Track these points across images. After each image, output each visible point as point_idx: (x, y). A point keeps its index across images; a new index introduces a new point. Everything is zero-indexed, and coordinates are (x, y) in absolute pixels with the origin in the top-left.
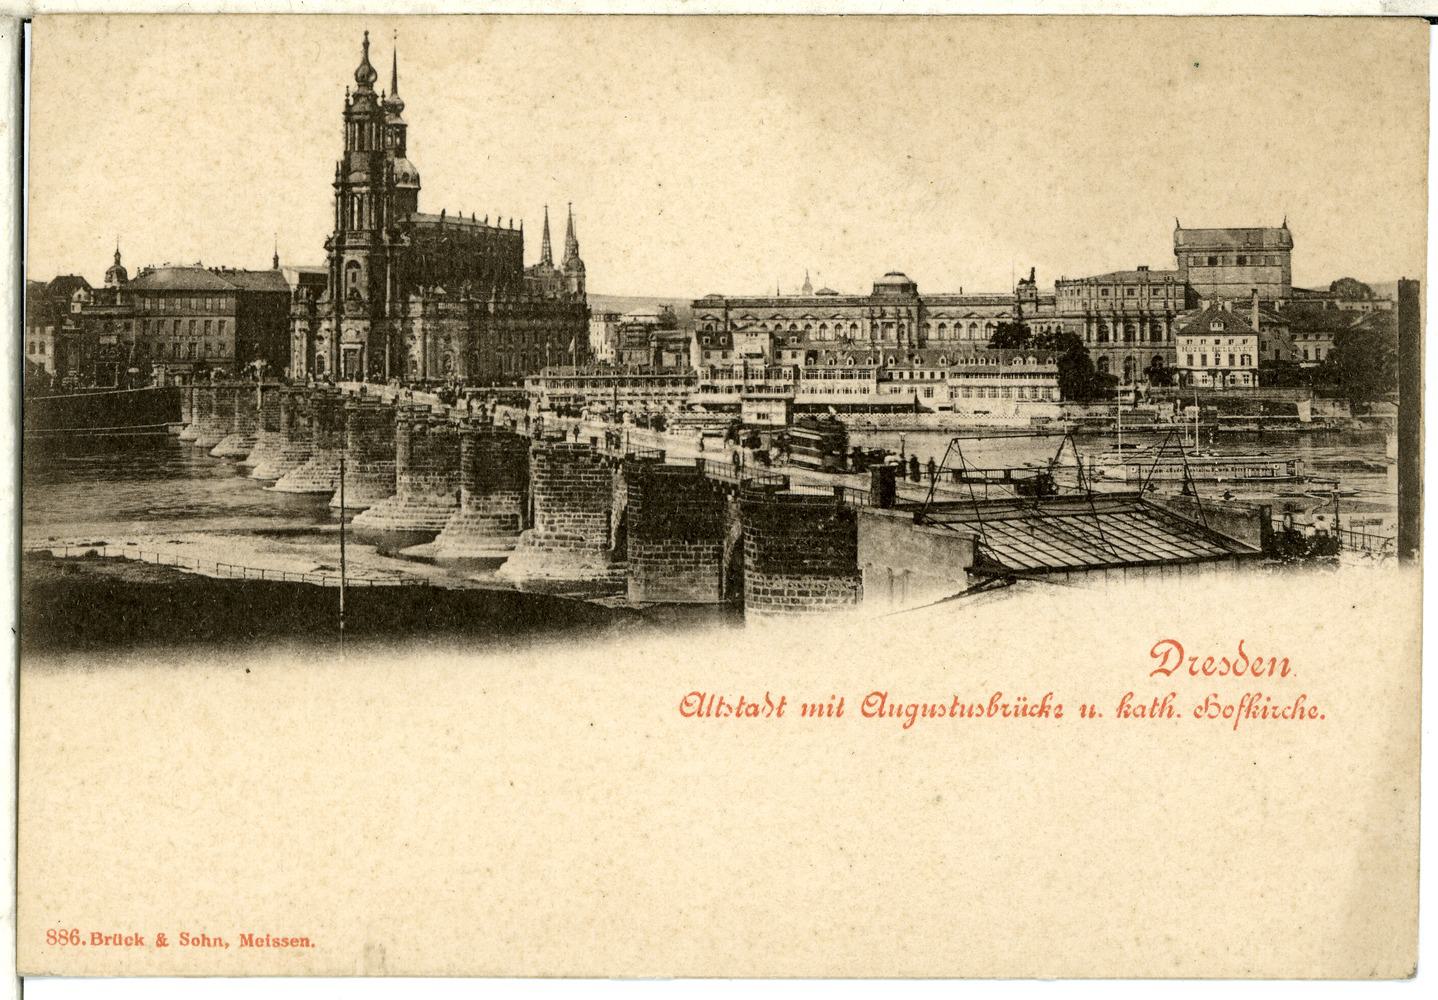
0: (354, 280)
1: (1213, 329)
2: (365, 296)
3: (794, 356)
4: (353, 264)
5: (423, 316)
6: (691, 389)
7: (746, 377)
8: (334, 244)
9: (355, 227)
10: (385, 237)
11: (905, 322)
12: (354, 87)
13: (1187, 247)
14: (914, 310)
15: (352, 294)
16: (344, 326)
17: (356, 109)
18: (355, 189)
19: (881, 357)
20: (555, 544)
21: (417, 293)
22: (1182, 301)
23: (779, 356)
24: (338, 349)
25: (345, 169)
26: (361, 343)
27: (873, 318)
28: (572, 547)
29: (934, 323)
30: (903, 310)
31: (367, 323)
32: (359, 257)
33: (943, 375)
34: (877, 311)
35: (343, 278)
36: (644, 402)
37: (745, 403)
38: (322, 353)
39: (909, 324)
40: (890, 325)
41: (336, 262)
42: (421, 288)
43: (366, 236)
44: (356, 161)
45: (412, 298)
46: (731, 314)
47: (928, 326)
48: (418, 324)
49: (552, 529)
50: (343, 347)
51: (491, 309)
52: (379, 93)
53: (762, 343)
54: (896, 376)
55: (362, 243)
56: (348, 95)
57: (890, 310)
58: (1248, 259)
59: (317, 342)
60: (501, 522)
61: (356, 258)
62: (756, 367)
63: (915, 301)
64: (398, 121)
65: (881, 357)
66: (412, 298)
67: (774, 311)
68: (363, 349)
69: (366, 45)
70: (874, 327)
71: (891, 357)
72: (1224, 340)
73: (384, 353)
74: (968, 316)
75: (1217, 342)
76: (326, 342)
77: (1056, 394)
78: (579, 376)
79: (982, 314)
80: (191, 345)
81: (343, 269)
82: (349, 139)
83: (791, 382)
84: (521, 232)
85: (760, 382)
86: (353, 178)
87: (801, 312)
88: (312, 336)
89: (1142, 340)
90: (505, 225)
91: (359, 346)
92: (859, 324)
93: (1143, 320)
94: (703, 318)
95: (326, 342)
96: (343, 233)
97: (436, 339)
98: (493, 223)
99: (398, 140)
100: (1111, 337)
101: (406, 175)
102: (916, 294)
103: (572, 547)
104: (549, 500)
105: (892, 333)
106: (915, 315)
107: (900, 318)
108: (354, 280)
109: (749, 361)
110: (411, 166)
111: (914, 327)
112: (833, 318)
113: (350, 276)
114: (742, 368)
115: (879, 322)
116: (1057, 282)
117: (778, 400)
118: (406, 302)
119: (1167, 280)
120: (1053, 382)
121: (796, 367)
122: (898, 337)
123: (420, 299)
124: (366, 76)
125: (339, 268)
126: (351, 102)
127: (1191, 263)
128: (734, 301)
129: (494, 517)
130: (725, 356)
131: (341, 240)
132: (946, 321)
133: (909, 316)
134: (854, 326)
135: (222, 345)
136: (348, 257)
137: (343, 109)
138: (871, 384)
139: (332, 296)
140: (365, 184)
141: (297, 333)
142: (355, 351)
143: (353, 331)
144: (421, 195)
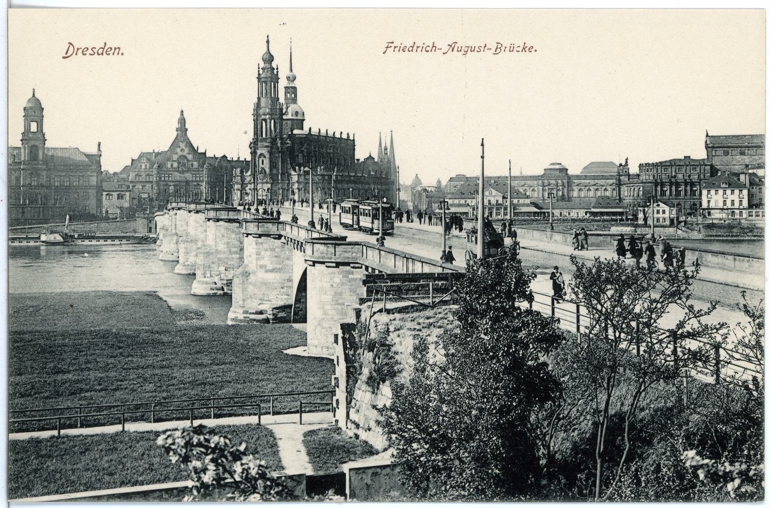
2: (268, 171)
8: (252, 145)
12: (262, 65)
17: (263, 76)
21: (295, 170)
25: (258, 106)
31: (269, 186)
32: (265, 151)
39: (563, 189)
41: (254, 153)
42: (297, 168)
45: (293, 173)
52: (275, 67)
61: (263, 152)
69: (268, 42)
76: (250, 196)
81: (257, 159)
82: (260, 93)
84: (354, 140)
86: (261, 111)
90: (344, 136)
96: (257, 139)
99: (293, 95)
102: (567, 174)
106: (566, 185)
113: (261, 161)
119: (700, 163)
125: (255, 157)
133: (563, 185)
136: (259, 152)
137: (257, 76)
144: (304, 122)
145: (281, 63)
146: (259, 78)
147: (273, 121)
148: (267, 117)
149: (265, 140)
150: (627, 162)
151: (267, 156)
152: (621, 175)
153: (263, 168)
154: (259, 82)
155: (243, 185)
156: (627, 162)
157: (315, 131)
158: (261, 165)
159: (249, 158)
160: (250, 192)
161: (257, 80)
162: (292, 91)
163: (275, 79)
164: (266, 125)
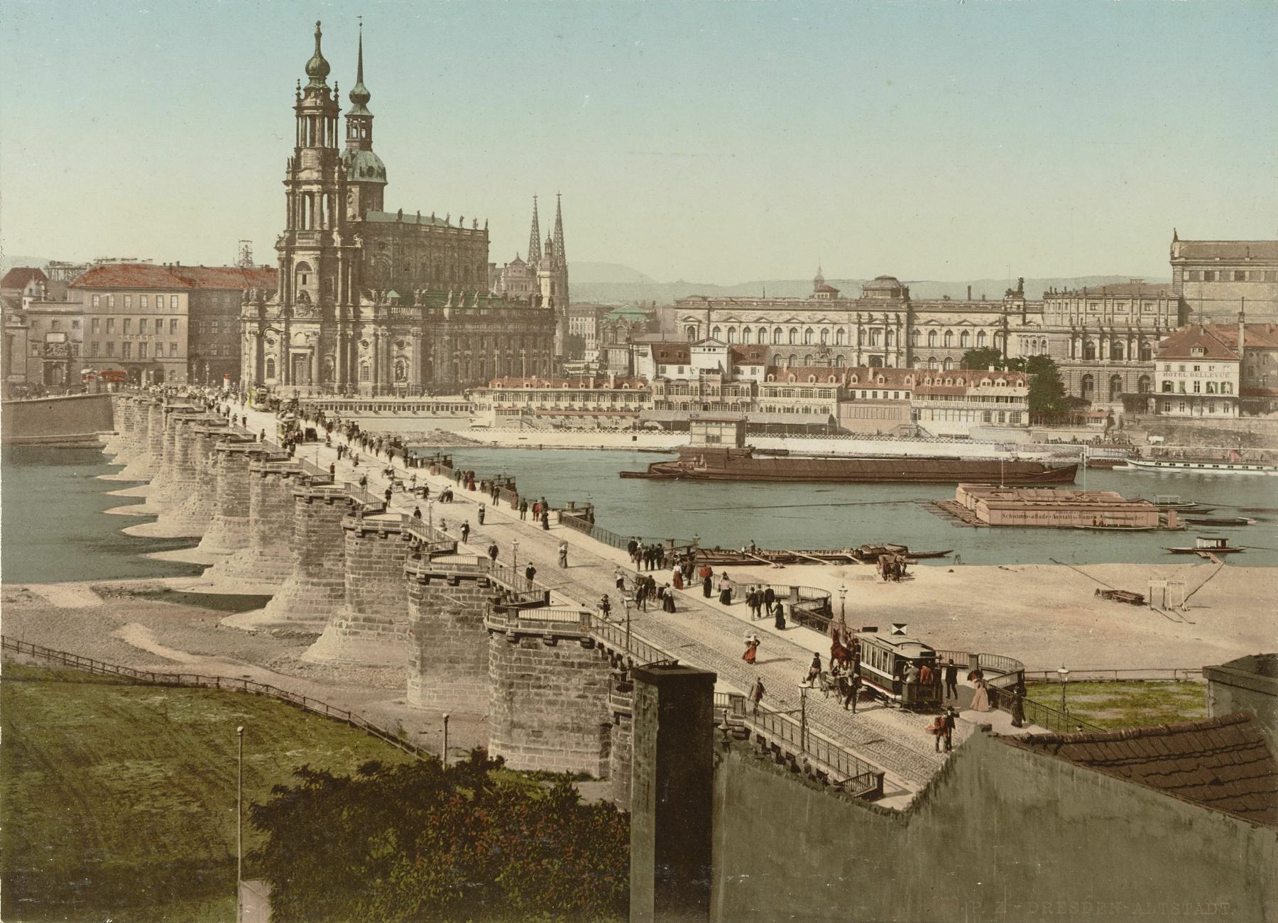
0: (304, 282)
1: (1193, 355)
2: (314, 298)
3: (753, 372)
4: (303, 265)
5: (375, 322)
6: (646, 405)
7: (702, 393)
8: (283, 244)
9: (307, 227)
10: (337, 238)
11: (894, 328)
12: (305, 81)
13: (1182, 260)
14: (903, 316)
15: (302, 296)
16: (293, 330)
18: (305, 188)
19: (844, 376)
20: (363, 627)
21: (368, 296)
22: (1176, 318)
23: (738, 371)
24: (288, 353)
25: (295, 166)
26: (311, 347)
27: (860, 324)
28: (380, 631)
29: (924, 331)
30: (892, 315)
32: (308, 257)
33: (907, 395)
34: (865, 315)
35: (293, 280)
36: (595, 417)
37: (694, 424)
38: (272, 356)
40: (878, 331)
41: (286, 262)
42: (373, 292)
43: (317, 236)
44: (309, 157)
45: (364, 302)
46: (714, 316)
47: (918, 332)
48: (368, 330)
49: (360, 611)
50: (292, 351)
51: (446, 312)
52: (333, 88)
53: (720, 358)
54: (858, 394)
55: (312, 243)
56: (299, 88)
57: (878, 315)
58: (1247, 274)
59: (266, 345)
60: (332, 590)
62: (711, 384)
63: (904, 307)
64: (365, 113)
65: (844, 376)
66: (364, 302)
67: (759, 314)
68: (312, 353)
69: (318, 36)
70: (860, 332)
71: (854, 376)
72: (1204, 366)
73: (334, 360)
74: (959, 324)
75: (1196, 368)
77: (1025, 419)
78: (529, 389)
79: (974, 322)
80: (141, 344)
82: (300, 136)
83: (748, 399)
85: (718, 399)
86: (303, 176)
87: (787, 315)
88: (261, 337)
89: (1129, 358)
90: (468, 225)
91: (309, 351)
92: (845, 328)
93: (1131, 337)
94: (685, 320)
95: (276, 347)
97: (389, 344)
98: (455, 223)
100: (1097, 355)
101: (371, 169)
103: (380, 631)
104: (358, 580)
105: (881, 339)
107: (888, 325)
108: (304, 282)
109: (705, 375)
110: (377, 160)
111: (903, 331)
112: (819, 322)
113: (300, 278)
114: (698, 384)
115: (866, 327)
116: (1046, 294)
117: (728, 422)
118: (356, 306)
120: (1024, 406)
121: (754, 383)
122: (887, 344)
123: (373, 303)
124: (319, 70)
125: (289, 268)
126: (302, 97)
127: (1186, 277)
128: (718, 302)
129: (325, 585)
130: (681, 371)
131: (291, 241)
132: (937, 328)
134: (841, 331)
135: (173, 346)
136: (298, 257)
138: (831, 403)
139: (282, 297)
140: (317, 182)
141: (247, 335)
142: (304, 355)
143: (303, 334)
145: (342, 80)
146: (299, 109)
147: (325, 196)
148: (315, 188)
149: (306, 235)
150: (1021, 287)
151: (313, 265)
152: (1010, 314)
153: (304, 294)
154: (297, 117)
155: (263, 322)
156: (1021, 287)
157: (410, 211)
158: (300, 286)
159: (275, 264)
160: (277, 338)
161: (294, 112)
162: (363, 122)
163: (331, 110)
164: (312, 205)
